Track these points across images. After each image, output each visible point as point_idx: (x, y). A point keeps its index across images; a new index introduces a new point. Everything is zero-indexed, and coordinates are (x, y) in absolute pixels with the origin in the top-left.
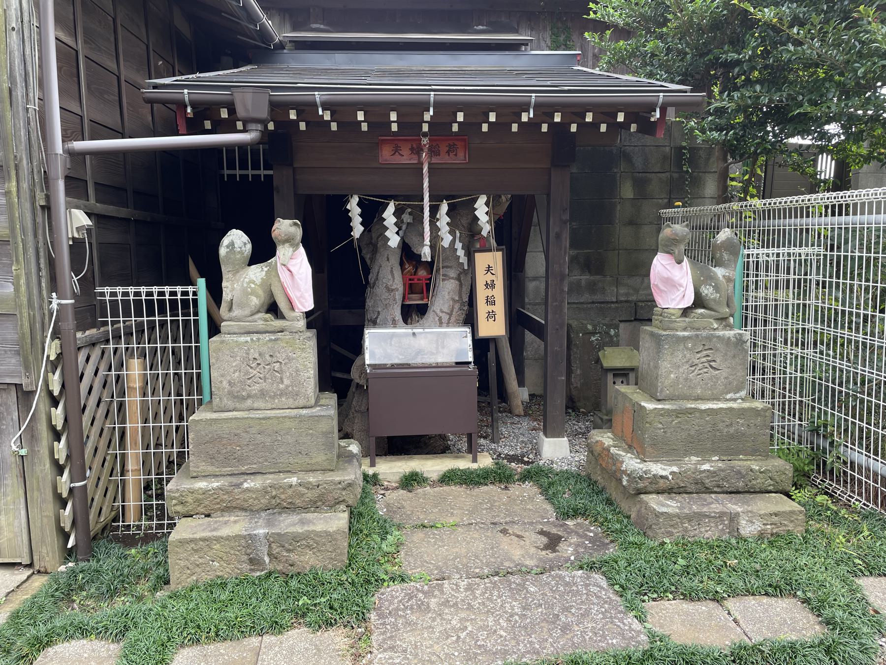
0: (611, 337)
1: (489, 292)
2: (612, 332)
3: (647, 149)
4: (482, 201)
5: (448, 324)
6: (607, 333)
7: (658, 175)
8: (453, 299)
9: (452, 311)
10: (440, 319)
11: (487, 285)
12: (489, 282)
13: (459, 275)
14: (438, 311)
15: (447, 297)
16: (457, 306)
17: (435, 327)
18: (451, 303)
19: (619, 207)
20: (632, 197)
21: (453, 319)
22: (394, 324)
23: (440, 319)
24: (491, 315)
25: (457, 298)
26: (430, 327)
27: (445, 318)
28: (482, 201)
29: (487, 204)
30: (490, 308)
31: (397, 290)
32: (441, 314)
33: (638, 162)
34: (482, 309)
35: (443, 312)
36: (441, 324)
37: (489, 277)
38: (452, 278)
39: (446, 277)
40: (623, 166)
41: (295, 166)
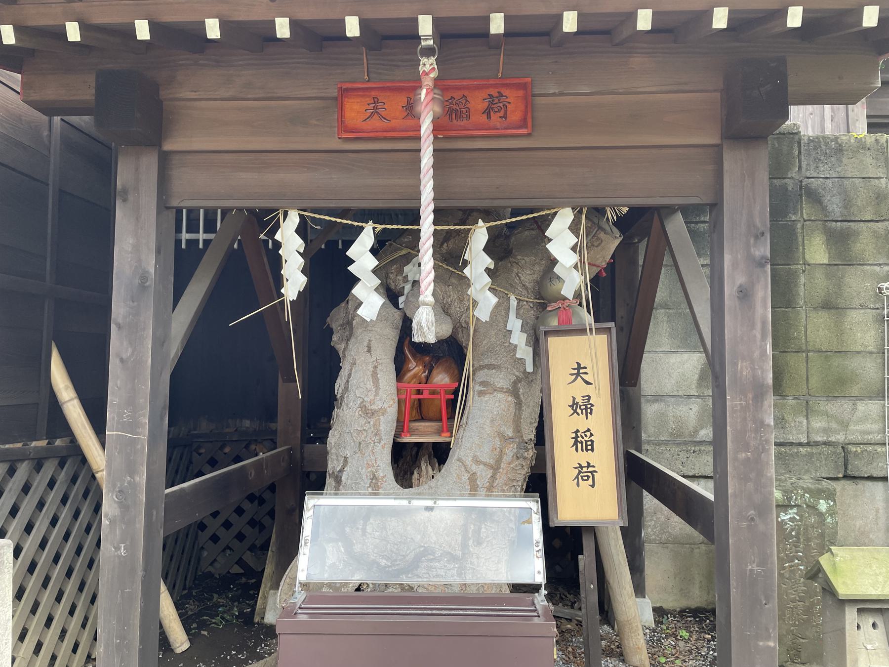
0: (821, 514)
1: (581, 423)
2: (823, 506)
3: (846, 182)
4: (563, 219)
5: (491, 491)
6: (813, 508)
7: (870, 224)
8: (501, 435)
9: (499, 461)
10: (473, 478)
11: (574, 405)
12: (579, 400)
13: (515, 383)
14: (469, 461)
15: (488, 429)
16: (510, 451)
17: (462, 497)
18: (498, 443)
19: (802, 280)
20: (826, 261)
21: (501, 479)
22: (375, 489)
23: (473, 478)
24: (585, 473)
25: (510, 433)
26: (449, 496)
27: (484, 475)
28: (563, 219)
29: (574, 228)
30: (584, 457)
31: (383, 412)
32: (474, 468)
33: (834, 206)
34: (564, 459)
35: (477, 462)
36: (474, 490)
37: (579, 390)
38: (501, 390)
39: (488, 388)
40: (807, 210)
41: (167, 147)
